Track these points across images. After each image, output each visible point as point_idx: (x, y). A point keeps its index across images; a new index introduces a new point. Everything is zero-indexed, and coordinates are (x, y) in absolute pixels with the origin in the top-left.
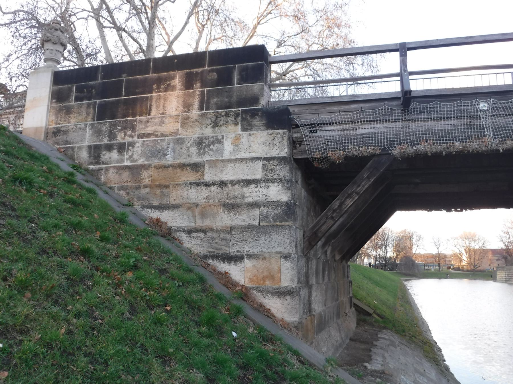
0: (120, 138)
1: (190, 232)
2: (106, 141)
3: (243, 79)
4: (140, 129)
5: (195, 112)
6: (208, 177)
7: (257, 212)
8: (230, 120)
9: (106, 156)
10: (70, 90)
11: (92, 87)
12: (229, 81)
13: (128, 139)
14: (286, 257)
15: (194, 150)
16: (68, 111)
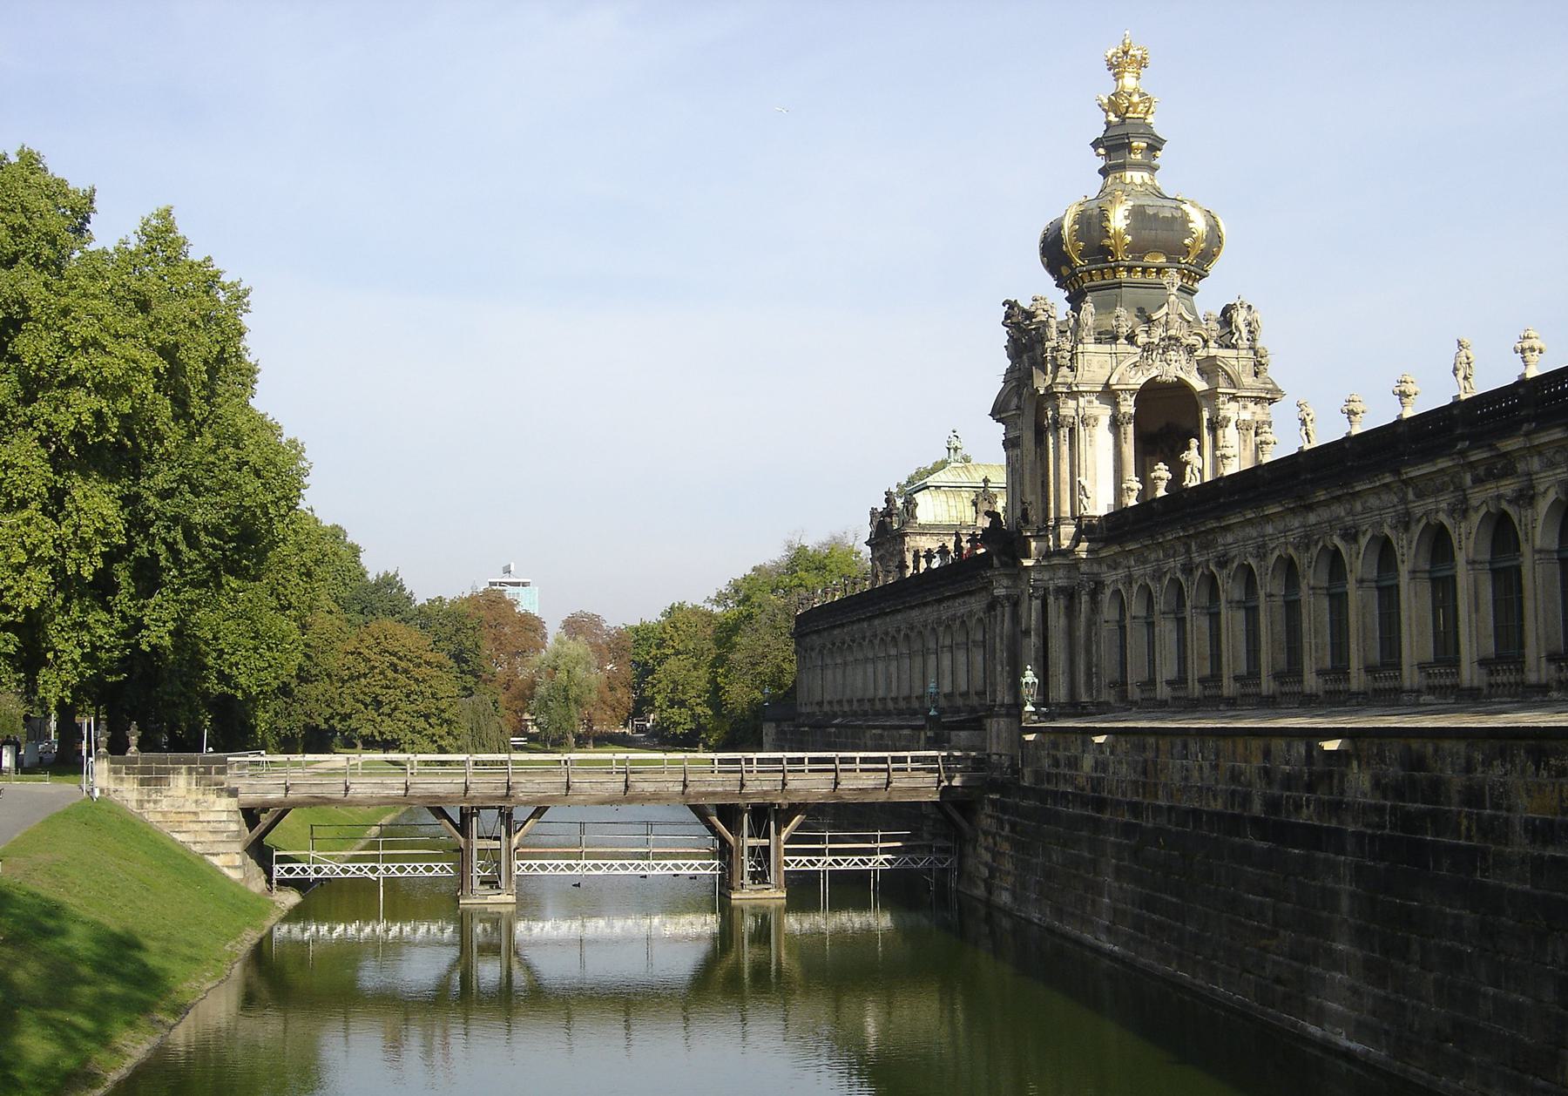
0: (154, 797)
1: (195, 843)
2: (146, 798)
3: (217, 773)
4: (165, 793)
5: (194, 787)
6: (200, 819)
7: (225, 835)
8: (212, 792)
9: (146, 805)
10: (122, 768)
11: (135, 768)
12: (210, 774)
13: (158, 798)
14: (238, 853)
15: (194, 805)
16: (122, 780)
